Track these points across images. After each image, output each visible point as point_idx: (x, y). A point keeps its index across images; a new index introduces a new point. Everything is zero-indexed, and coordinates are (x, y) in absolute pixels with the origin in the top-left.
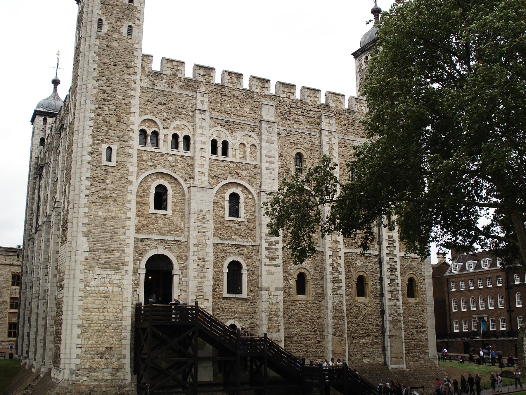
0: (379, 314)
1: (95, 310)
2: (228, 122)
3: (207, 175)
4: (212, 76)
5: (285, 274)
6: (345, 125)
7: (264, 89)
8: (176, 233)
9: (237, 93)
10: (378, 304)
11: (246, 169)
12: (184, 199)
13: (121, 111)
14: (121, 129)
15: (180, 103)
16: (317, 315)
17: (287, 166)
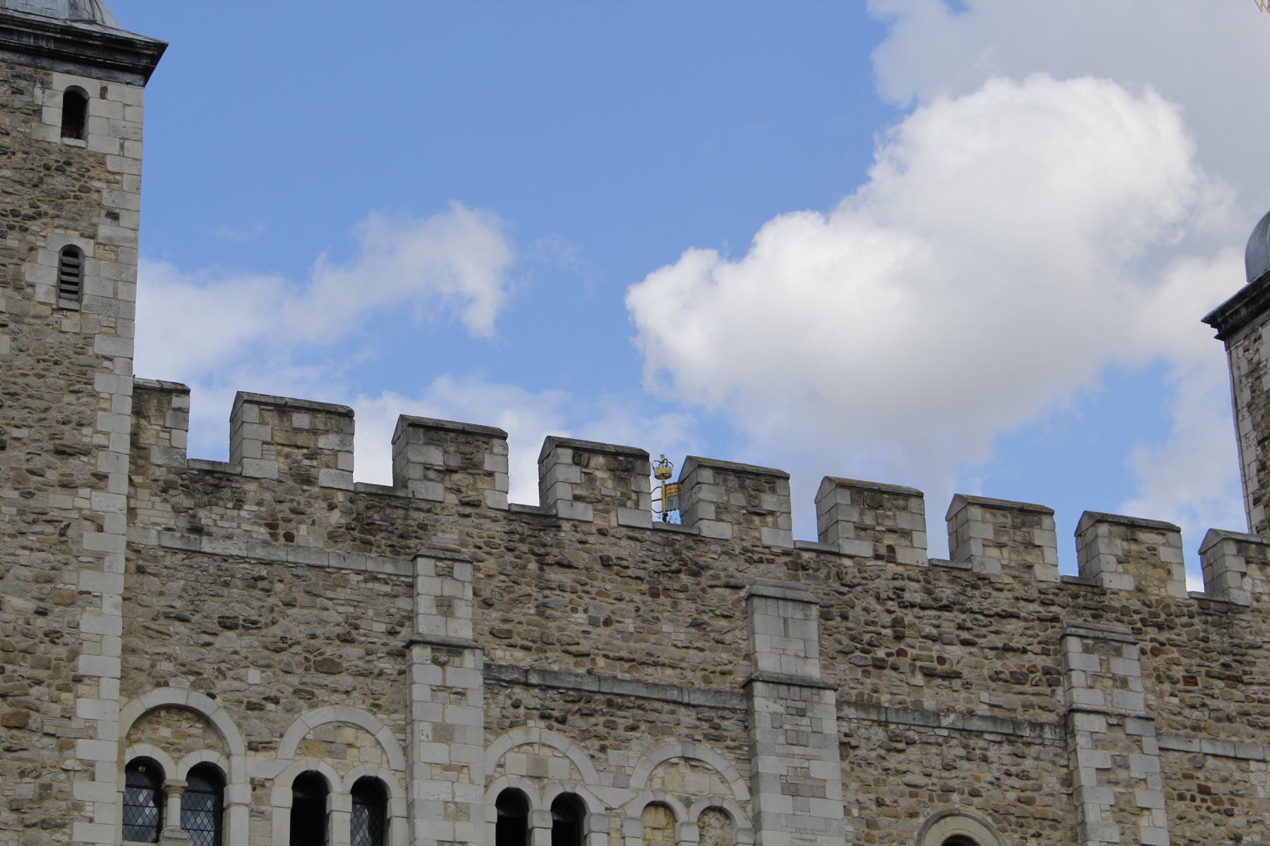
4: (491, 474)
6: (1190, 680)
7: (756, 519)
9: (623, 549)
14: (29, 765)
15: (332, 616)
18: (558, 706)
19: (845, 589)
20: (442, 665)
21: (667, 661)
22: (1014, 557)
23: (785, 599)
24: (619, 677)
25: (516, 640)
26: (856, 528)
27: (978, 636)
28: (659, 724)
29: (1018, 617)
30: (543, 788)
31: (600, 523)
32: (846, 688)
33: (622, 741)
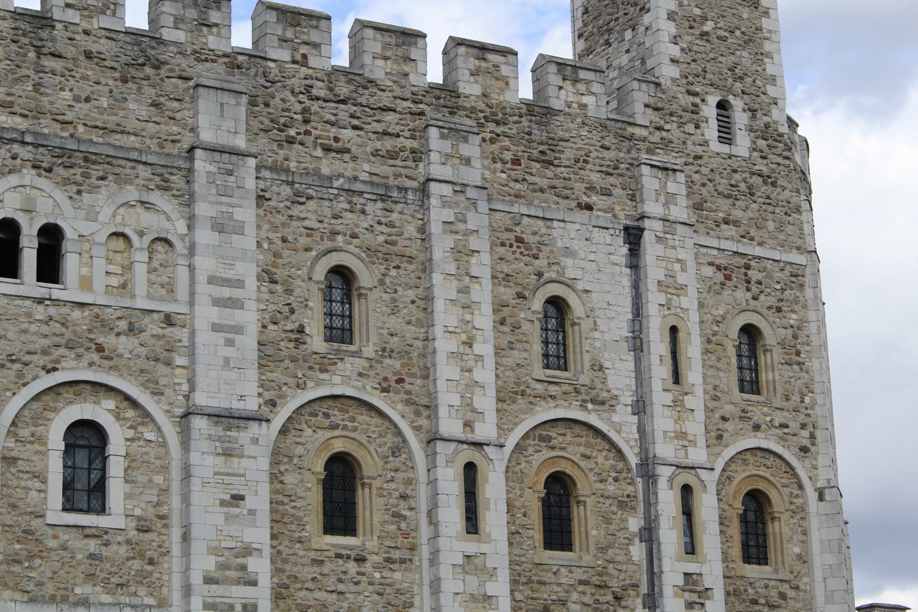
2: (63, 154)
6: (516, 162)
7: (205, 29)
9: (103, 46)
17: (294, 317)
19: (269, 84)
21: (131, 131)
22: (395, 67)
23: (223, 89)
24: (94, 140)
25: (16, 109)
26: (279, 39)
27: (364, 123)
28: (123, 176)
29: (395, 111)
30: (32, 219)
31: (85, 25)
32: (265, 157)
33: (94, 187)
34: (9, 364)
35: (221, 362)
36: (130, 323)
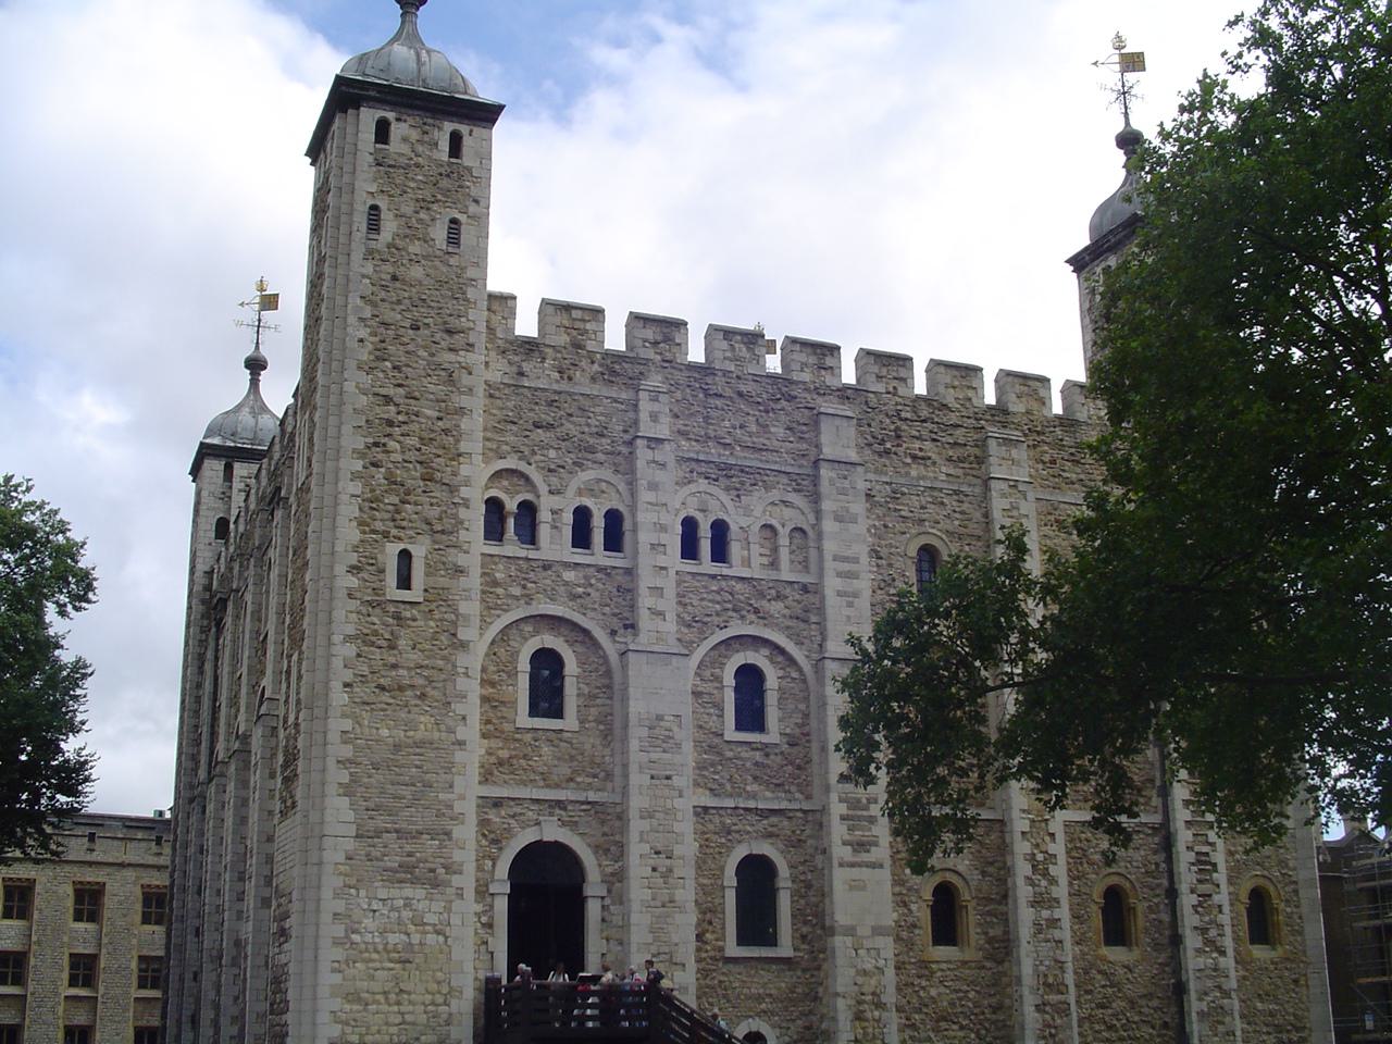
0: (1170, 994)
1: (378, 997)
2: (725, 469)
3: (671, 616)
4: (679, 345)
5: (897, 889)
6: (1053, 462)
7: (823, 372)
8: (590, 780)
10: (1167, 965)
11: (779, 597)
12: (609, 687)
13: (434, 451)
14: (434, 501)
16: (993, 1001)
18: (713, 472)
20: (653, 449)
30: (706, 516)
34: (694, 624)
35: (844, 619)
36: (778, 592)
